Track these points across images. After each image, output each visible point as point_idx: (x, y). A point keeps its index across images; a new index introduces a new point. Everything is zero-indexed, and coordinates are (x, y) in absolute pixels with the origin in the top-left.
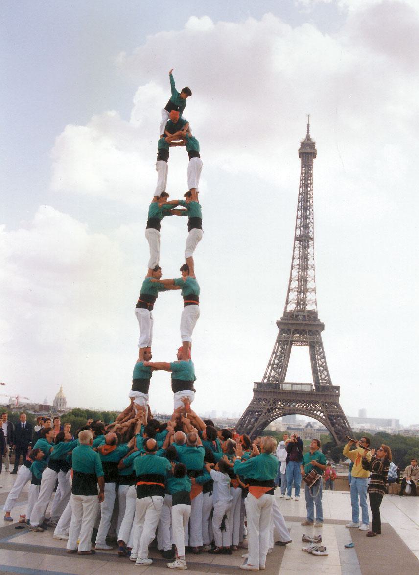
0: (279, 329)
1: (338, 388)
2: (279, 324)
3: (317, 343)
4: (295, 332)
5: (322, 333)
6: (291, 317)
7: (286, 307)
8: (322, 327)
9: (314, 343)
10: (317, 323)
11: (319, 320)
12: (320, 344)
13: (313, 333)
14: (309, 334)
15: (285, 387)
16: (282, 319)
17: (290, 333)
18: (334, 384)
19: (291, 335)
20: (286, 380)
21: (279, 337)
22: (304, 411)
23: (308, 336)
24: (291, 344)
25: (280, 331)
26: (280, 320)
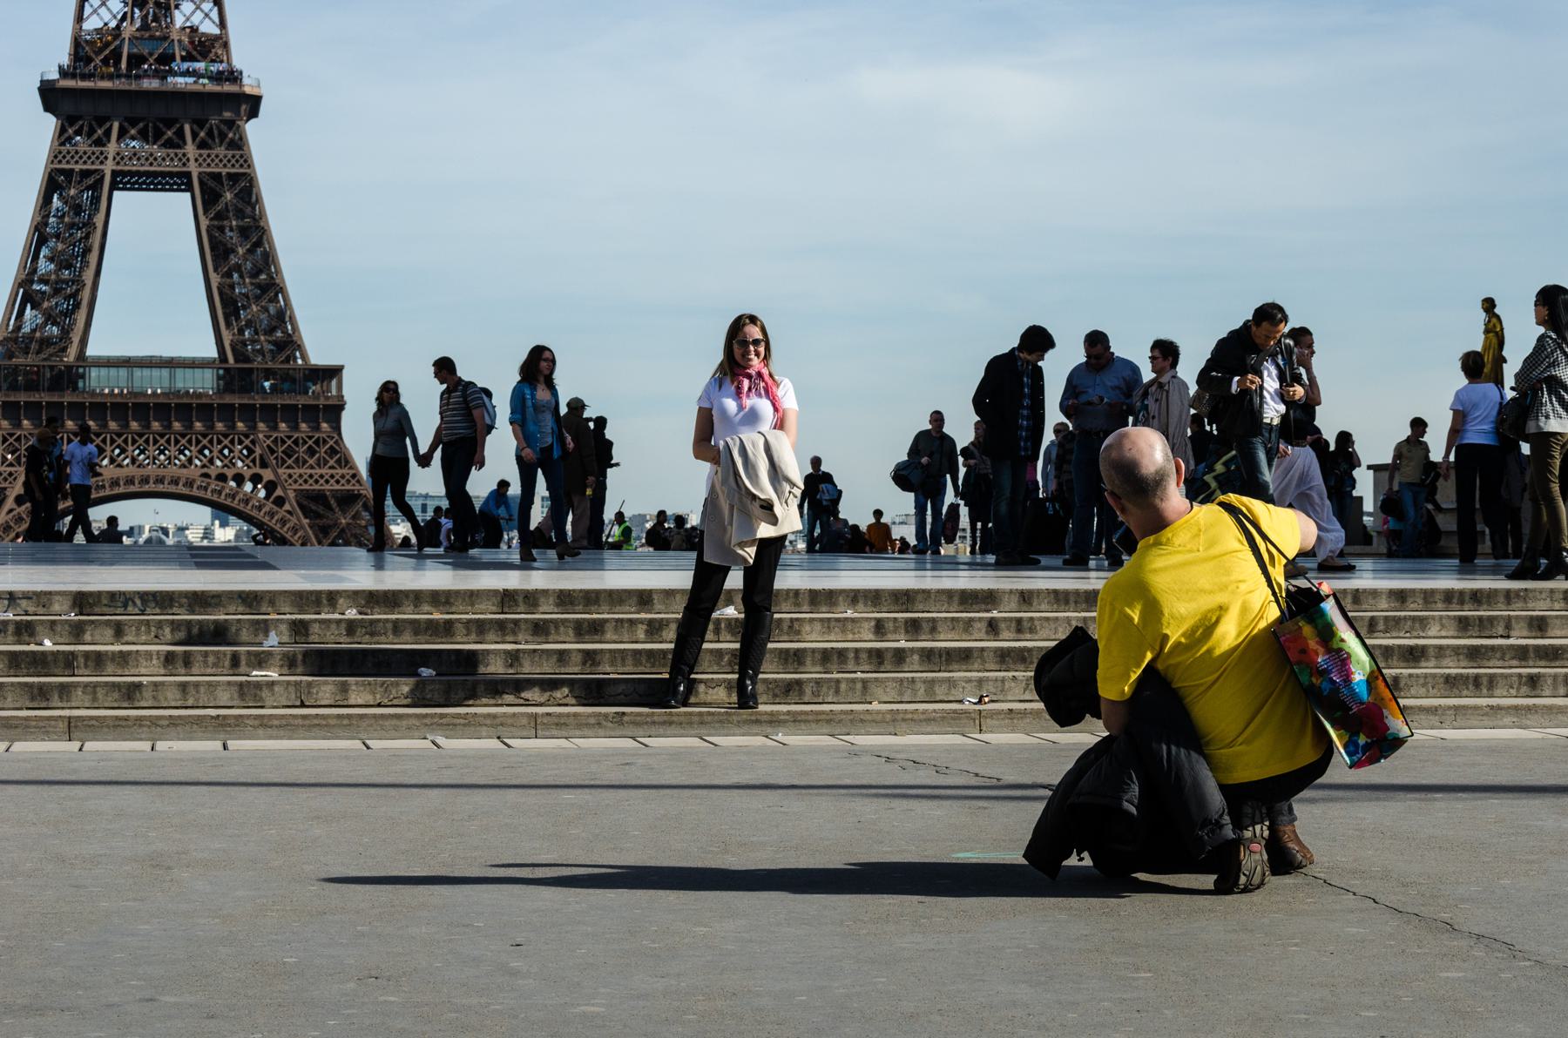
0: (50, 123)
1: (334, 372)
2: (50, 95)
3: (234, 178)
4: (133, 132)
5: (252, 129)
6: (105, 62)
7: (80, 18)
8: (252, 105)
9: (217, 177)
10: (228, 88)
11: (234, 76)
12: (245, 186)
13: (210, 134)
14: (195, 135)
15: (99, 381)
16: (64, 73)
17: (108, 133)
18: (318, 352)
19: (112, 148)
20: (92, 350)
21: (55, 156)
22: (190, 483)
23: (190, 149)
24: (114, 187)
25: (62, 137)
26: (55, 75)
